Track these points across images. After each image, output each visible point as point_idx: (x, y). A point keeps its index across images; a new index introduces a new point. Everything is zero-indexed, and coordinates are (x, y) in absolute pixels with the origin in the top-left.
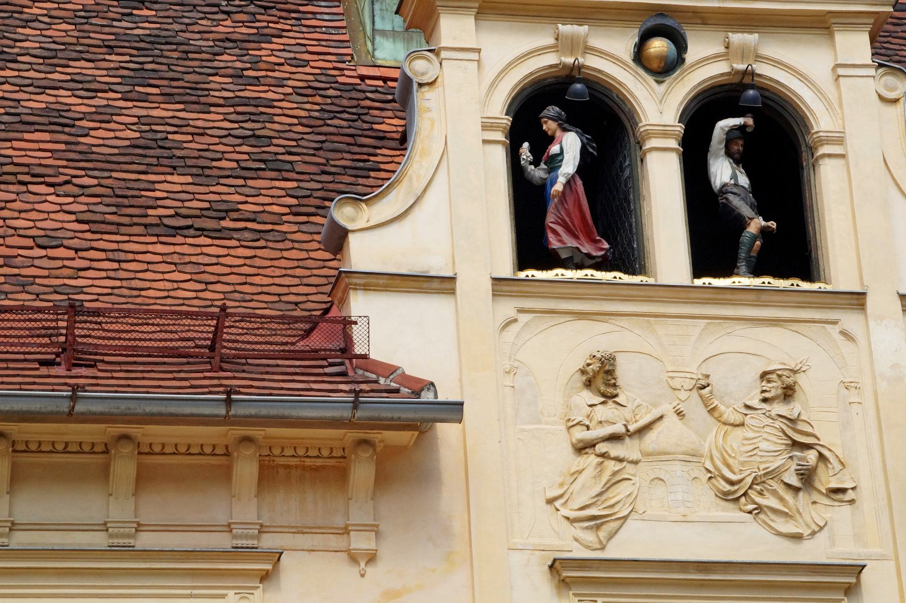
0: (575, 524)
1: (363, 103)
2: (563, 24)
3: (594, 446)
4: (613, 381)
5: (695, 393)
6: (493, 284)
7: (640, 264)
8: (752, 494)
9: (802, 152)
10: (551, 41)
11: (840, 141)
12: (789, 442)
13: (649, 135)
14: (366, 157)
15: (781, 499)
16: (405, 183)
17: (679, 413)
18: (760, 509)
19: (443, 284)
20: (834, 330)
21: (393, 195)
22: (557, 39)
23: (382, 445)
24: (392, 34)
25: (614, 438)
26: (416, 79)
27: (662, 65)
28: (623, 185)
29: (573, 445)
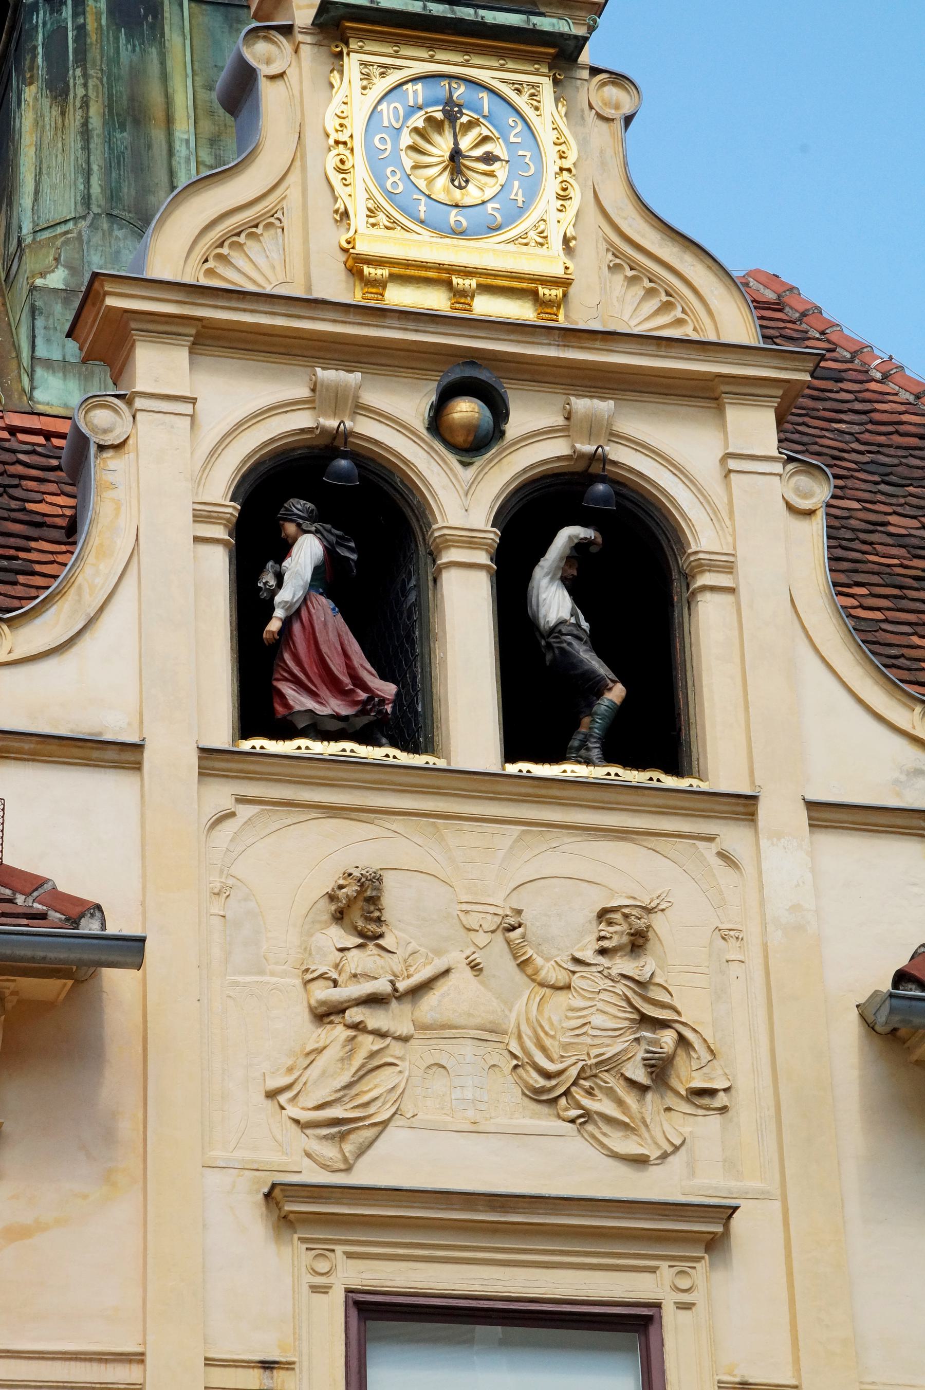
0: (308, 1131)
1: (12, 469)
2: (323, 369)
3: (343, 1011)
4: (377, 914)
5: (499, 937)
6: (199, 758)
7: (426, 738)
8: (577, 1093)
9: (672, 581)
10: (304, 392)
11: (728, 568)
12: (636, 1016)
13: (448, 542)
14: (12, 552)
15: (620, 1103)
16: (72, 594)
17: (475, 967)
18: (587, 1116)
19: (125, 755)
20: (708, 850)
21: (50, 615)
22: (313, 390)
23: (15, 999)
24: (63, 367)
25: (374, 1001)
26: (95, 439)
27: (471, 438)
28: (405, 615)
29: (312, 1010)
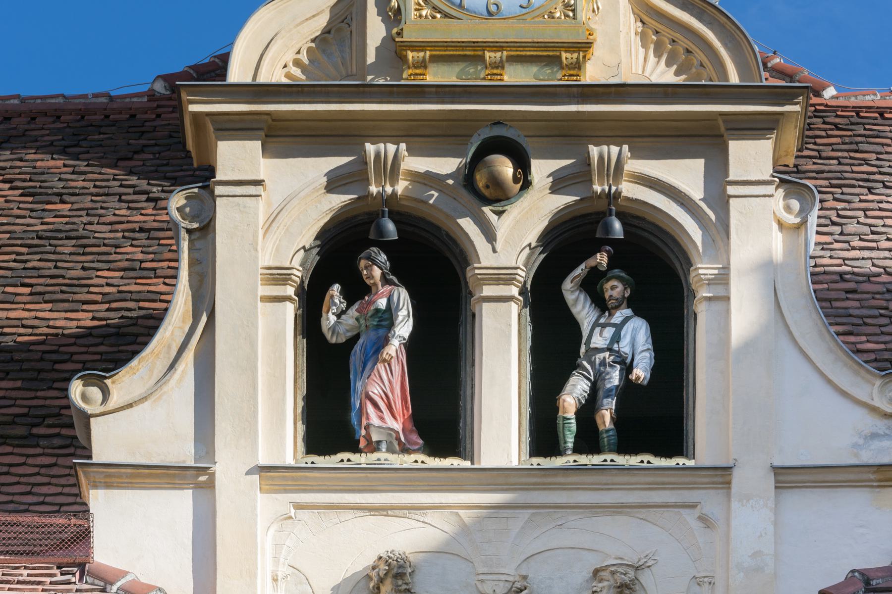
4: (404, 587)
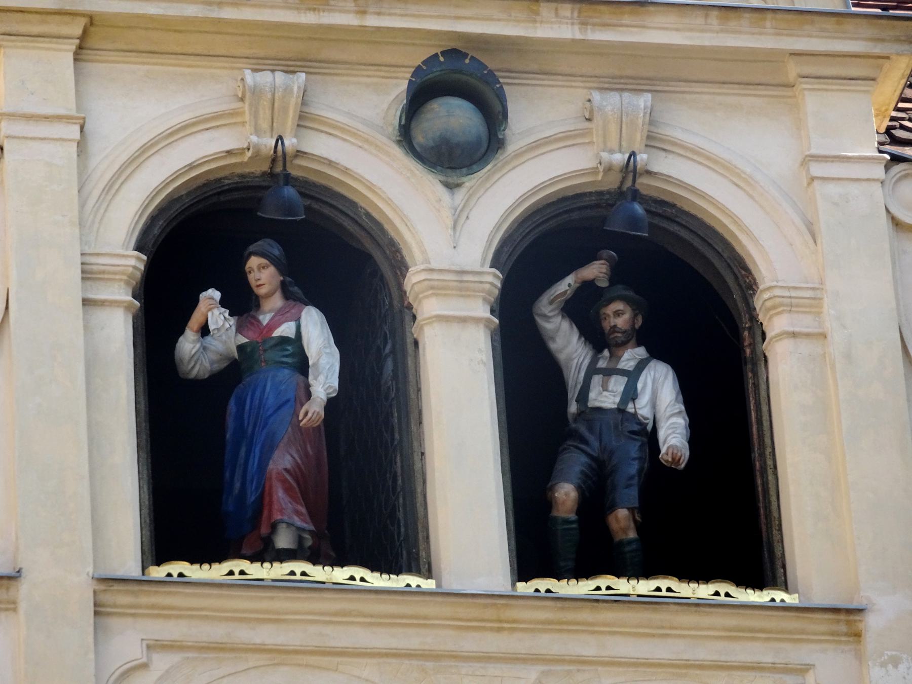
2: (255, 70)
11: (814, 305)
